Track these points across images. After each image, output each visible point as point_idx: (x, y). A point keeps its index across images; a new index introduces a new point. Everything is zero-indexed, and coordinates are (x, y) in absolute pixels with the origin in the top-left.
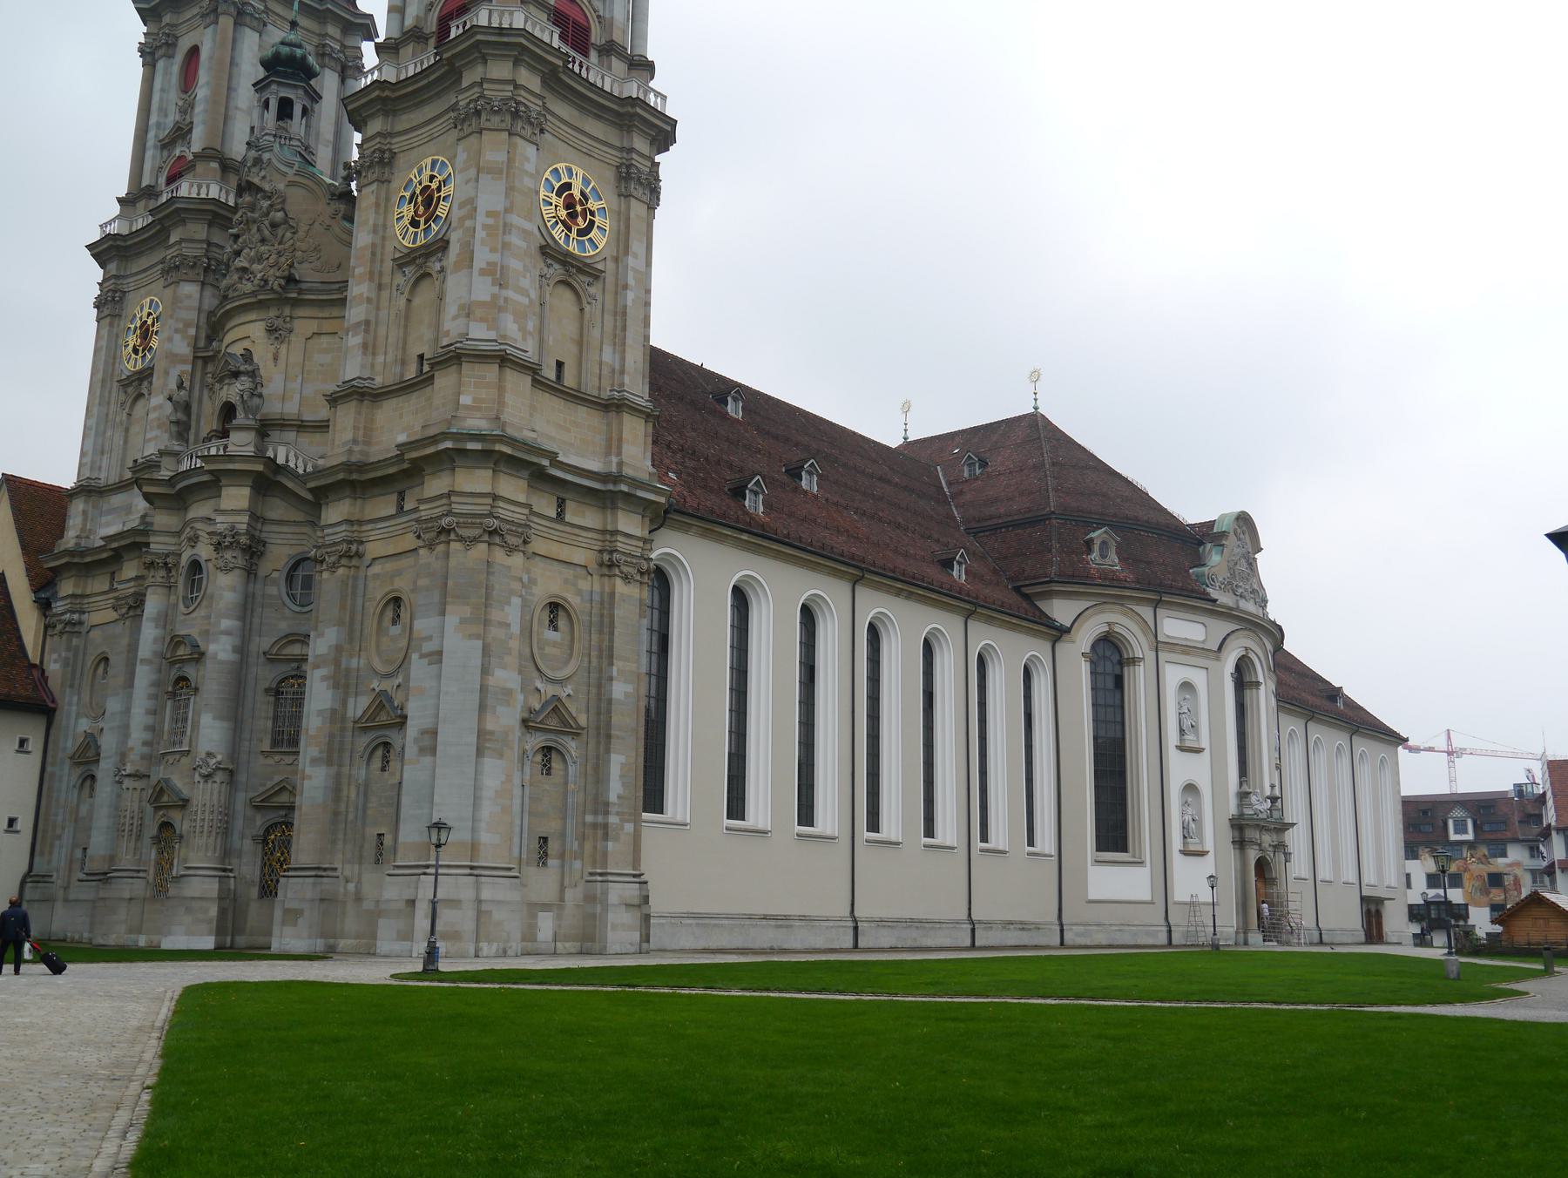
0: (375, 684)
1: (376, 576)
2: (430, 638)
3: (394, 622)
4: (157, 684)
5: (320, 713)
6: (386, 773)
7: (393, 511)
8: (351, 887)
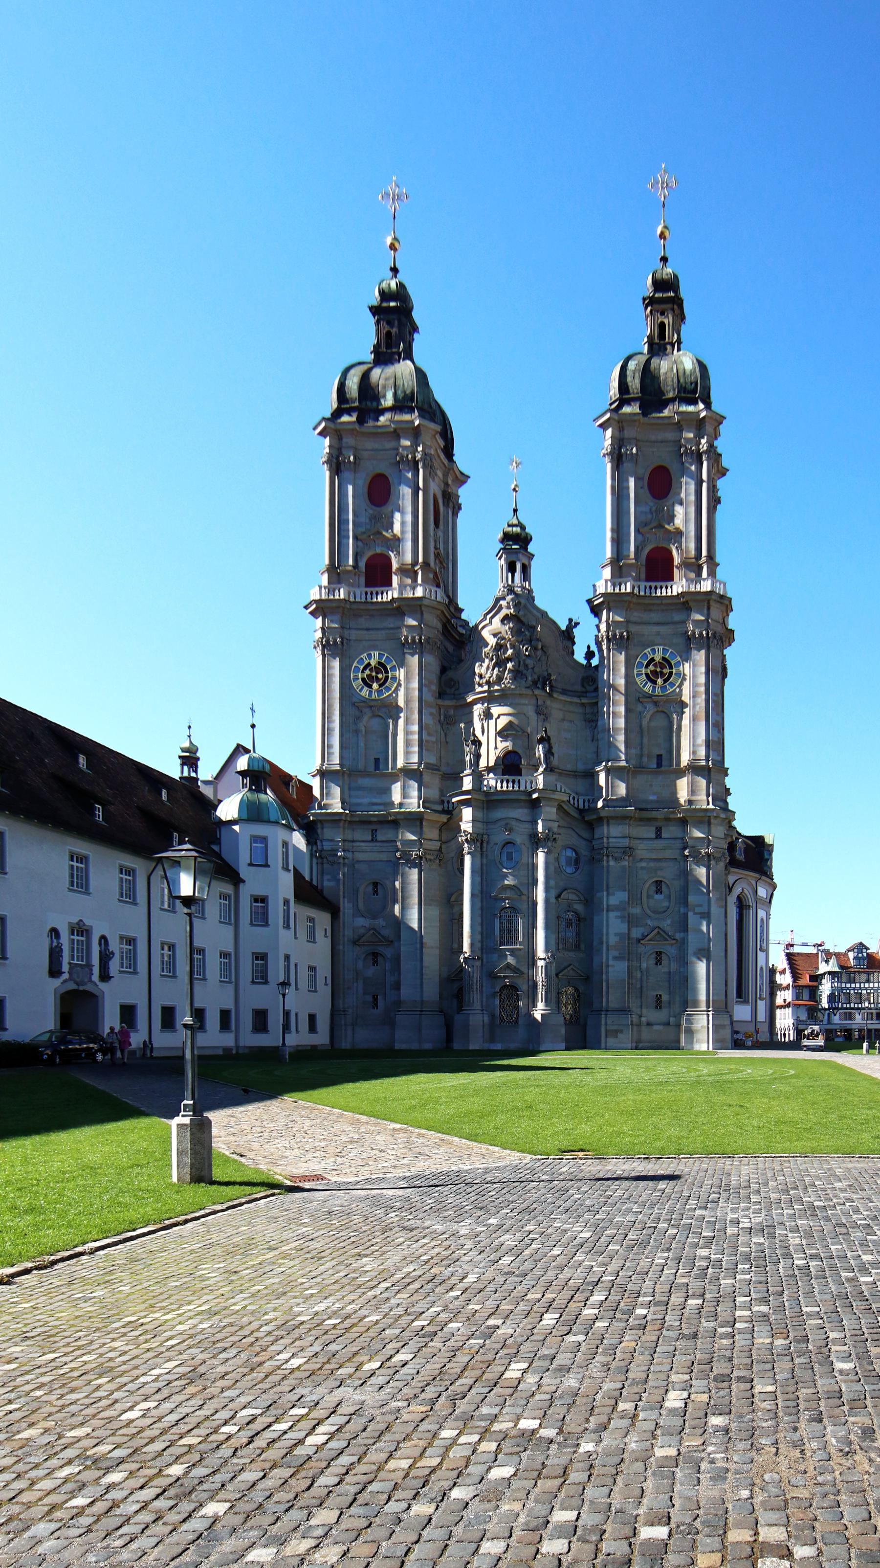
0: (649, 922)
1: (642, 868)
2: (700, 906)
3: (657, 893)
4: (482, 909)
5: (616, 934)
6: (660, 967)
7: (654, 836)
8: (643, 1019)
